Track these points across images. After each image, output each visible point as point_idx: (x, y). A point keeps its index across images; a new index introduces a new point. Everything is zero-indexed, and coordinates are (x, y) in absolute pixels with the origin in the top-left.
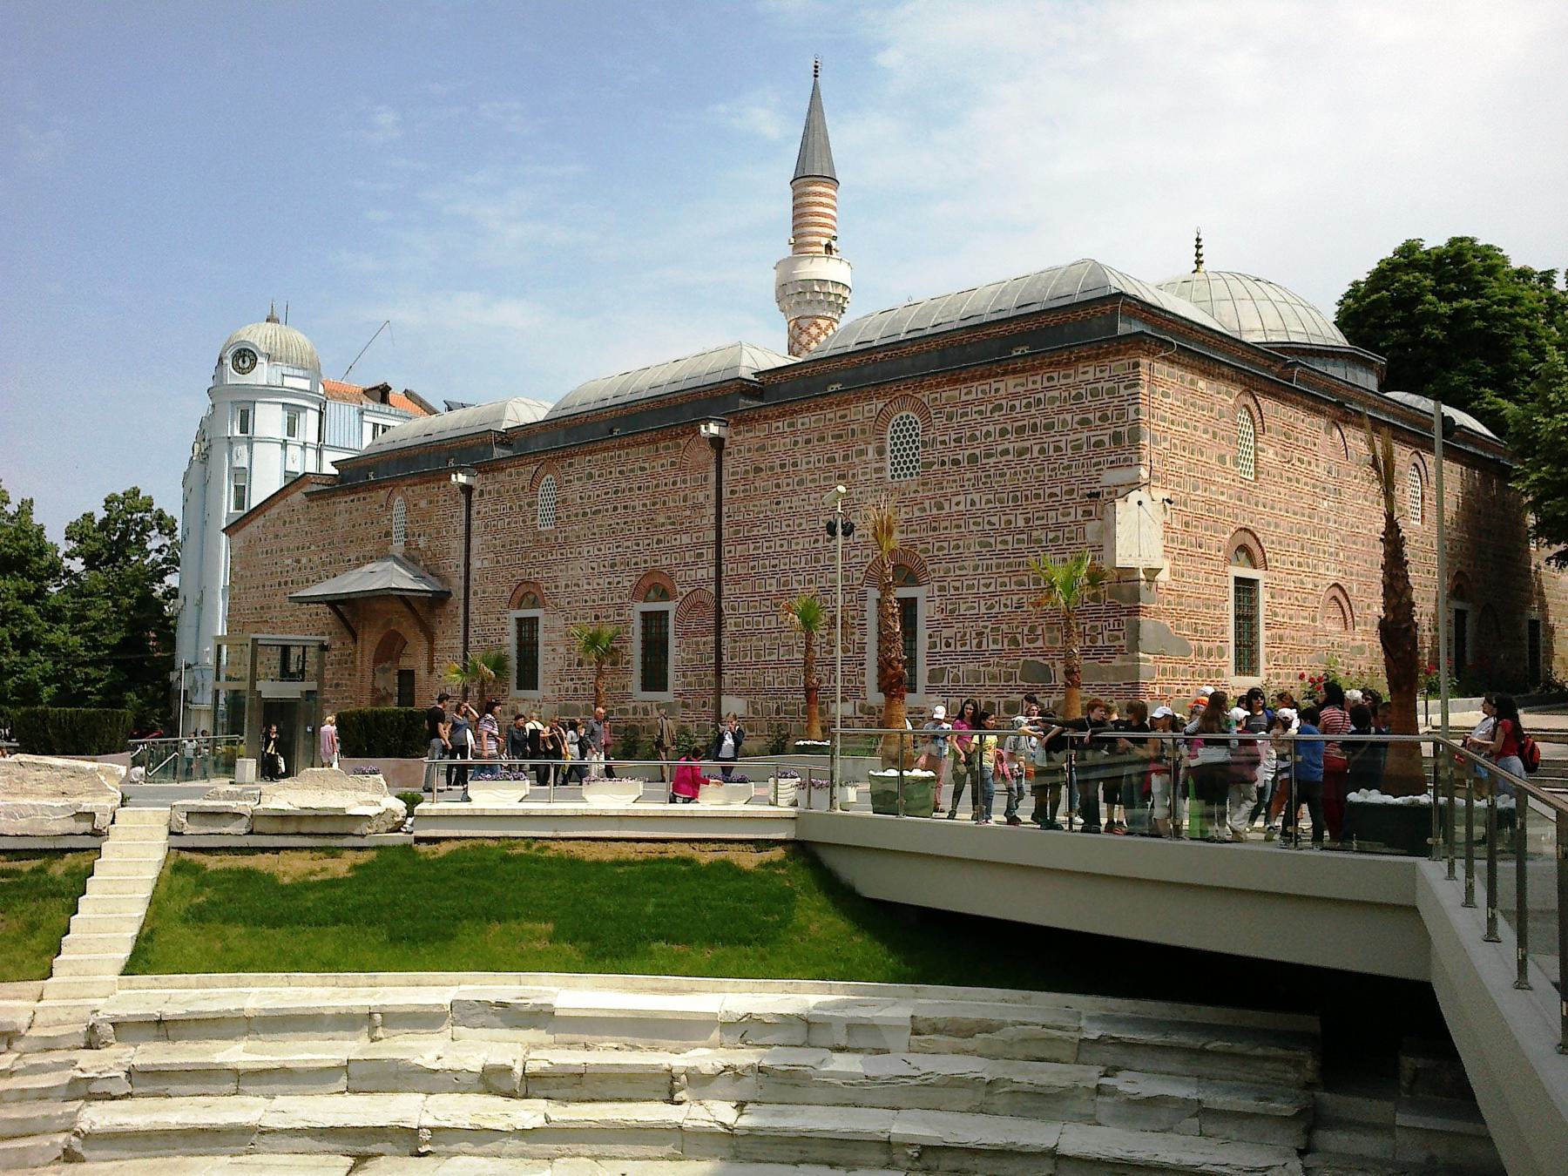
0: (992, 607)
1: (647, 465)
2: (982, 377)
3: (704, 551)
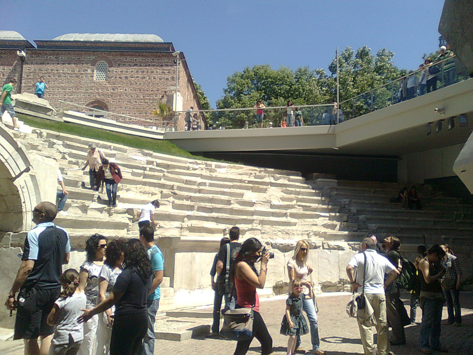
2: (132, 55)
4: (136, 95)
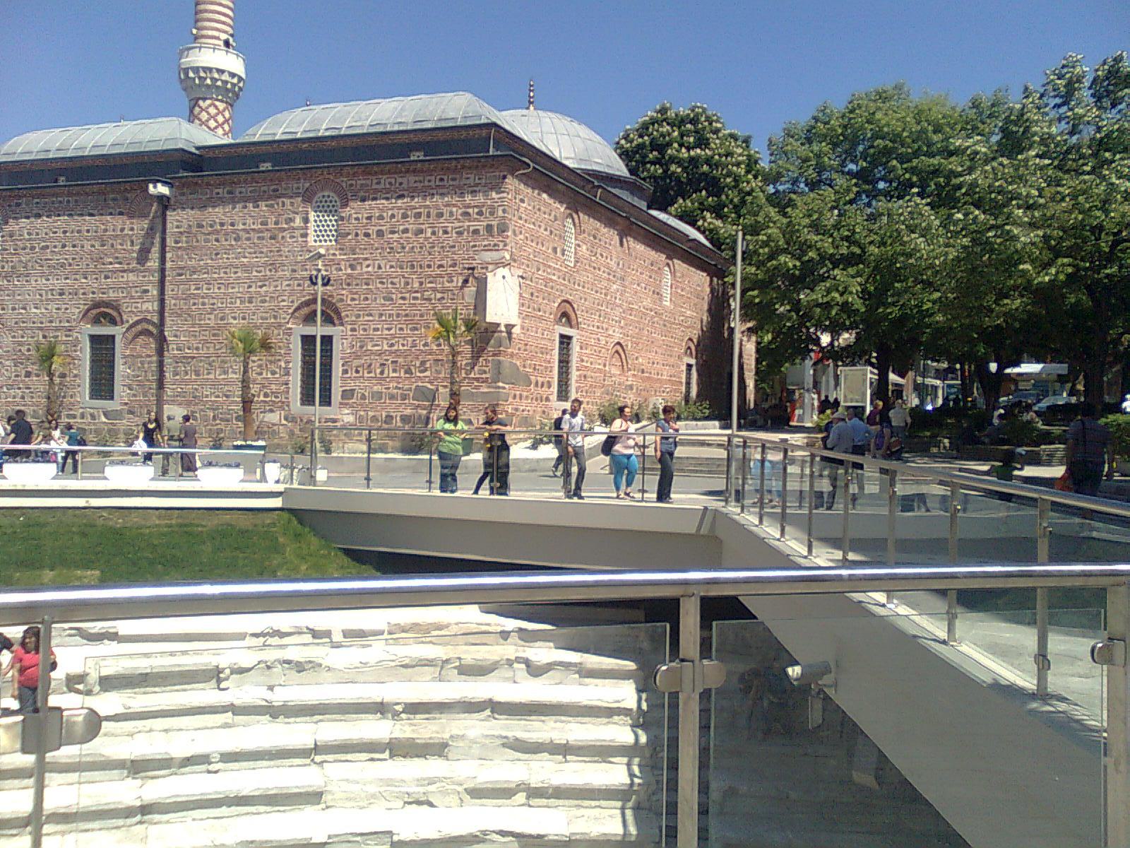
0: (392, 345)
2: (389, 172)
3: (149, 288)
4: (403, 280)
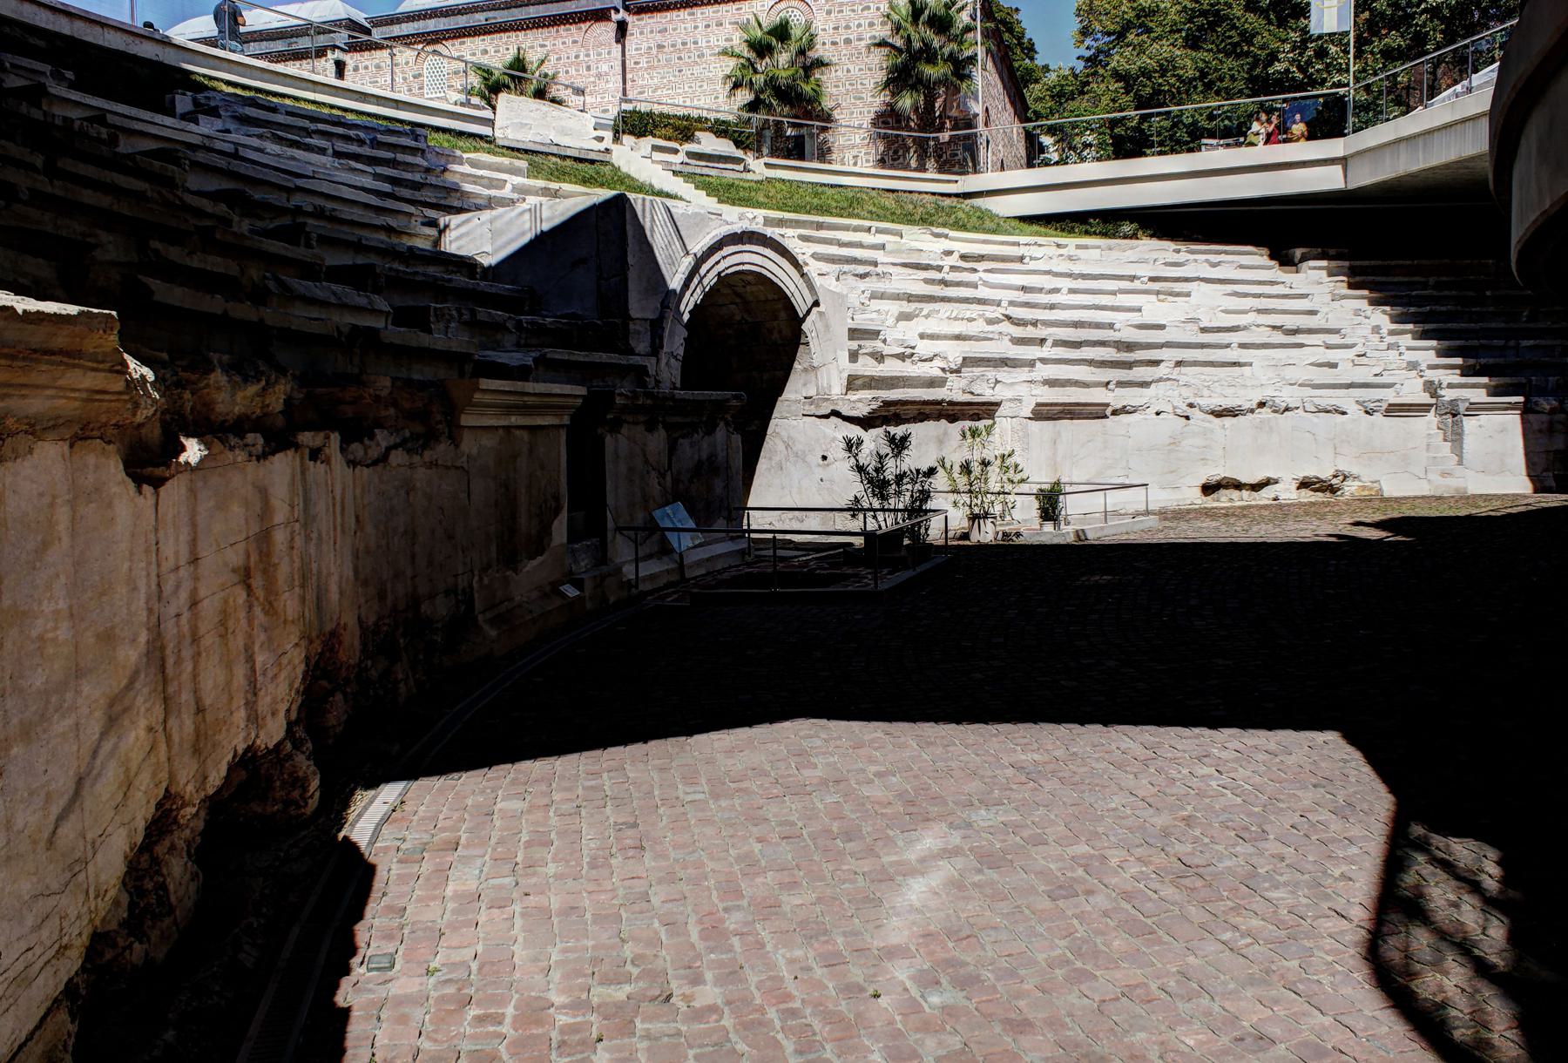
1: (547, 43)
